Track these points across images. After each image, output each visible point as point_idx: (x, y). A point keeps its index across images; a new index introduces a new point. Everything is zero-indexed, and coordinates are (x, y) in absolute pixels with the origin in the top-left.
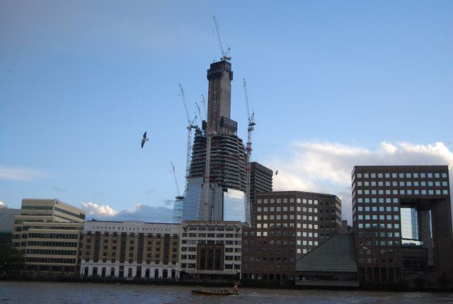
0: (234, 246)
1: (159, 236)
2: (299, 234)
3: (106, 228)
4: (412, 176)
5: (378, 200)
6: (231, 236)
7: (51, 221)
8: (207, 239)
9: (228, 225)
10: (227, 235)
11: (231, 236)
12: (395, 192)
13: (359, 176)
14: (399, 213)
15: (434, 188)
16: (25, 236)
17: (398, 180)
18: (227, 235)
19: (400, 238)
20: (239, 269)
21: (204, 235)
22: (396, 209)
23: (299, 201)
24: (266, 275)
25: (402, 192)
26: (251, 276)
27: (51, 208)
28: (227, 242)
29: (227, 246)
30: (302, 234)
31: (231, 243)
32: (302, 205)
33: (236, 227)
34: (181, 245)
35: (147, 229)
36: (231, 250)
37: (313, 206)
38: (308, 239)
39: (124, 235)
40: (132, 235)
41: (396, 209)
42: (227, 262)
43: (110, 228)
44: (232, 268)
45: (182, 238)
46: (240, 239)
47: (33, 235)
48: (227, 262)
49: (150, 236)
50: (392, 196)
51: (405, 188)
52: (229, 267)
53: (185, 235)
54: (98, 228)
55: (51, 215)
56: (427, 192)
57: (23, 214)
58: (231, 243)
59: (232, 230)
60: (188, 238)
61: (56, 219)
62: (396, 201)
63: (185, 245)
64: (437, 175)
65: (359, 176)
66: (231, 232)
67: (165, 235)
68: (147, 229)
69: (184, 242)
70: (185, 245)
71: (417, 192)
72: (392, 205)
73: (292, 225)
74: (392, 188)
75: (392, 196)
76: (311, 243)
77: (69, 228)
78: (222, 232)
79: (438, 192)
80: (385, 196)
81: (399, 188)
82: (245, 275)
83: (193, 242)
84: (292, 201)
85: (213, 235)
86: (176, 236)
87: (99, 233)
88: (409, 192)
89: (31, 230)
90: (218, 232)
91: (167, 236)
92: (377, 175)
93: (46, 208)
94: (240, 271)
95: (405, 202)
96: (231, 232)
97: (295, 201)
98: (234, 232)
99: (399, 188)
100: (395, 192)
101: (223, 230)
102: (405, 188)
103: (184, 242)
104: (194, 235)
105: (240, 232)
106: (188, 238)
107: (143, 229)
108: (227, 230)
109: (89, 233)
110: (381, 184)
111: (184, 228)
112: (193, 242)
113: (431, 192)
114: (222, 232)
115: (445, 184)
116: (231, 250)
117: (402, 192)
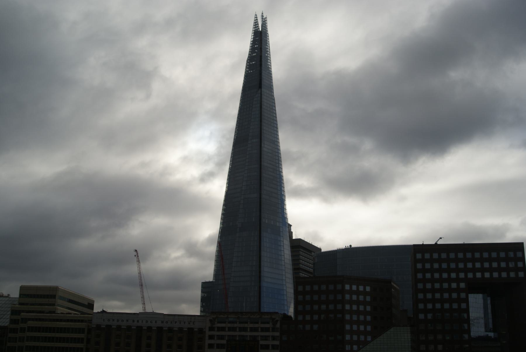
0: (270, 342)
1: (181, 330)
2: (348, 327)
3: (118, 321)
6: (267, 330)
7: (54, 312)
8: (237, 333)
10: (263, 330)
11: (267, 330)
12: (462, 275)
13: (419, 256)
14: (466, 301)
15: (508, 270)
16: (23, 330)
18: (263, 330)
19: (468, 331)
21: (234, 329)
22: (463, 295)
23: (347, 287)
25: (470, 275)
27: (54, 297)
28: (262, 336)
29: (262, 342)
30: (351, 327)
31: (266, 338)
34: (208, 342)
35: (167, 322)
37: (365, 293)
39: (139, 328)
40: (150, 329)
41: (463, 295)
43: (123, 321)
45: (208, 333)
46: (277, 334)
47: (32, 329)
49: (170, 330)
50: (458, 280)
53: (211, 329)
54: (109, 320)
55: (54, 305)
56: (500, 275)
57: (20, 304)
58: (266, 338)
59: (268, 323)
60: (215, 333)
61: (60, 310)
62: (462, 285)
63: (212, 342)
64: (511, 254)
65: (419, 256)
66: (267, 326)
67: (189, 329)
68: (167, 322)
69: (211, 337)
70: (212, 342)
71: (487, 275)
72: (458, 290)
73: (339, 316)
74: (457, 270)
75: (458, 280)
77: (75, 321)
78: (256, 326)
81: (466, 270)
83: (221, 337)
84: (339, 287)
85: (244, 329)
86: (201, 331)
87: (110, 326)
88: (479, 275)
89: (31, 323)
90: (252, 325)
91: (191, 330)
93: (47, 296)
95: (474, 287)
96: (267, 326)
97: (343, 287)
99: (466, 270)
100: (462, 275)
101: (257, 323)
102: (474, 270)
103: (211, 337)
104: (223, 329)
105: (278, 325)
106: (215, 333)
107: (162, 322)
108: (262, 323)
109: (98, 327)
111: (211, 321)
112: (221, 337)
113: (504, 275)
114: (256, 326)
117: (470, 275)
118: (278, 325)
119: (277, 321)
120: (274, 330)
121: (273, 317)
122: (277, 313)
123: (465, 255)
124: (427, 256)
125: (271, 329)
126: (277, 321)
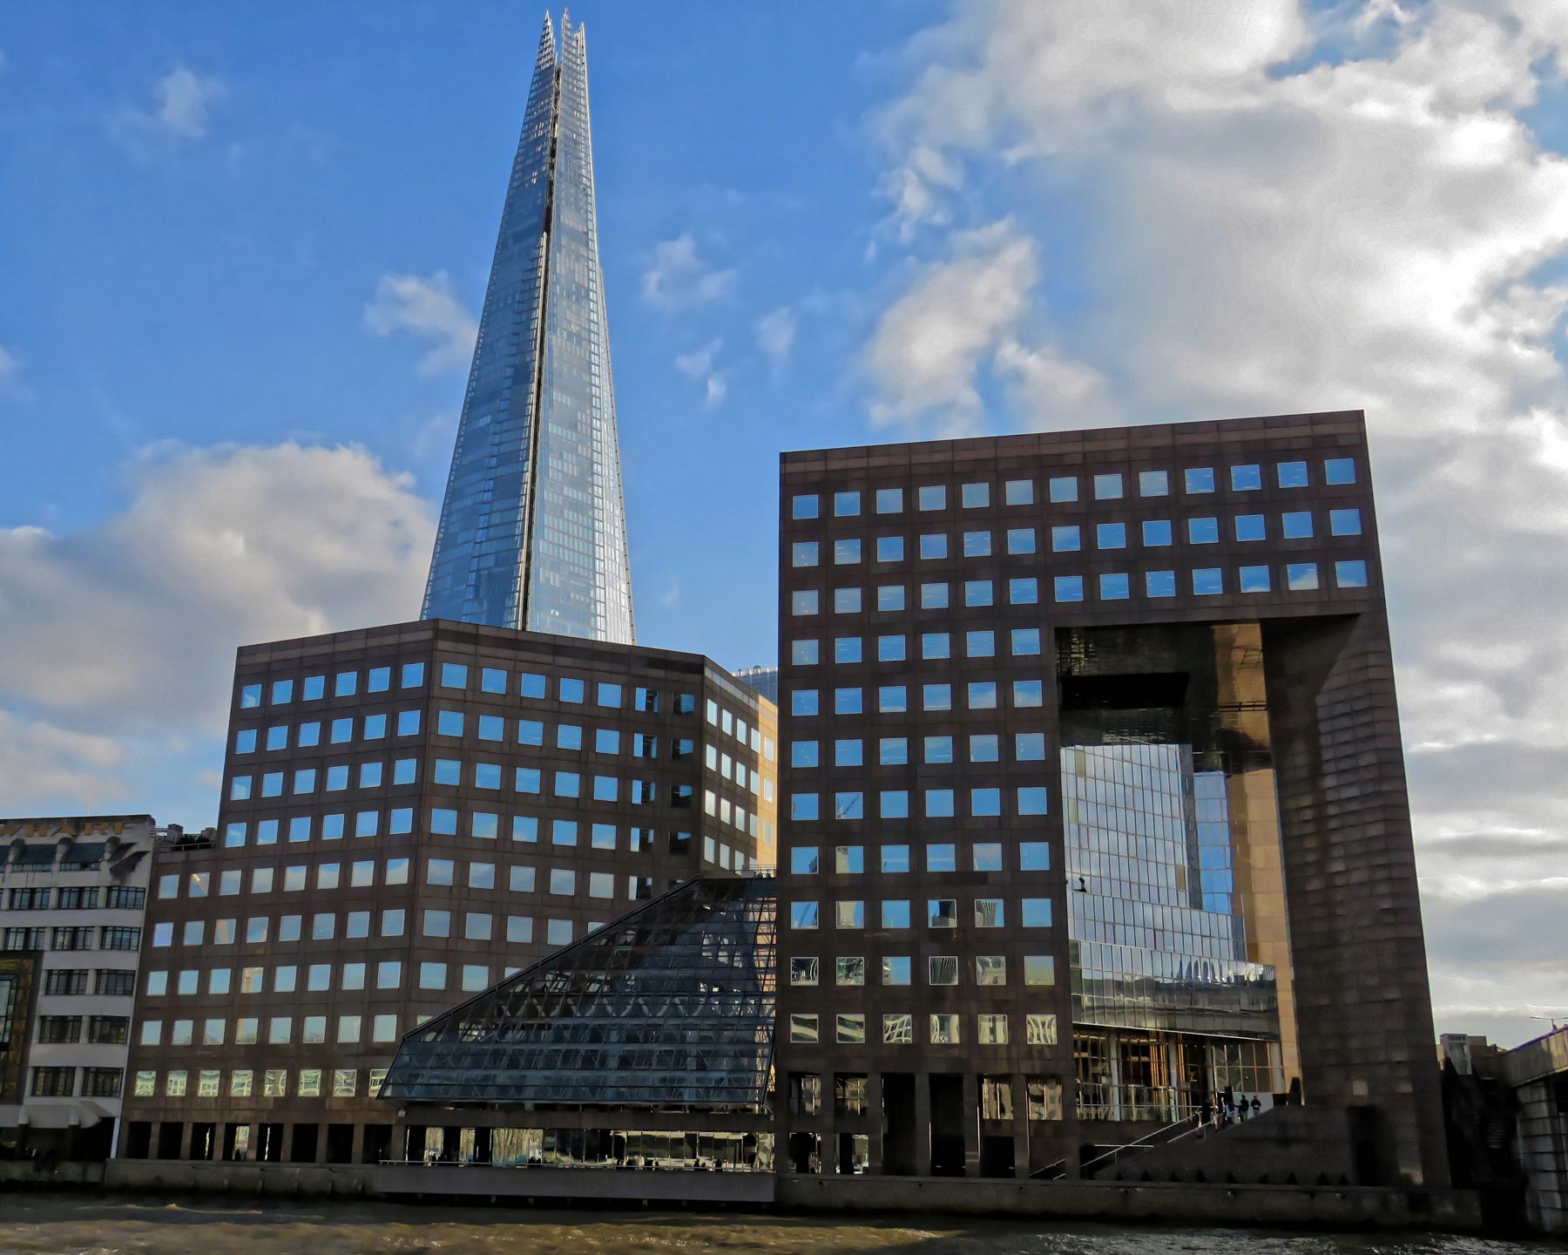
4: (1131, 485)
5: (914, 647)
6: (78, 898)
9: (83, 839)
11: (78, 898)
12: (1024, 591)
13: (807, 507)
17: (1043, 515)
20: (111, 1093)
24: (278, 1129)
25: (1068, 588)
26: (231, 1130)
29: (54, 961)
32: (472, 702)
33: (119, 848)
36: (68, 981)
38: (500, 903)
42: (42, 1053)
44: (68, 1092)
48: (42, 1053)
51: (1087, 562)
52: (55, 1080)
58: (75, 938)
65: (807, 507)
74: (1003, 567)
76: (520, 930)
78: (38, 879)
79: (1304, 580)
80: (955, 620)
82: (138, 1135)
88: (1114, 586)
92: (910, 499)
94: (112, 1107)
97: (431, 675)
98: (99, 877)
99: (1046, 566)
102: (1087, 562)
110: (936, 647)
113: (1254, 581)
114: (38, 879)
115: (1343, 522)
116: (68, 981)
118: (140, 877)
119: (140, 855)
120: (116, 896)
121: (125, 838)
122: (146, 820)
123: (1041, 489)
124: (847, 503)
125: (102, 892)
126: (140, 855)
